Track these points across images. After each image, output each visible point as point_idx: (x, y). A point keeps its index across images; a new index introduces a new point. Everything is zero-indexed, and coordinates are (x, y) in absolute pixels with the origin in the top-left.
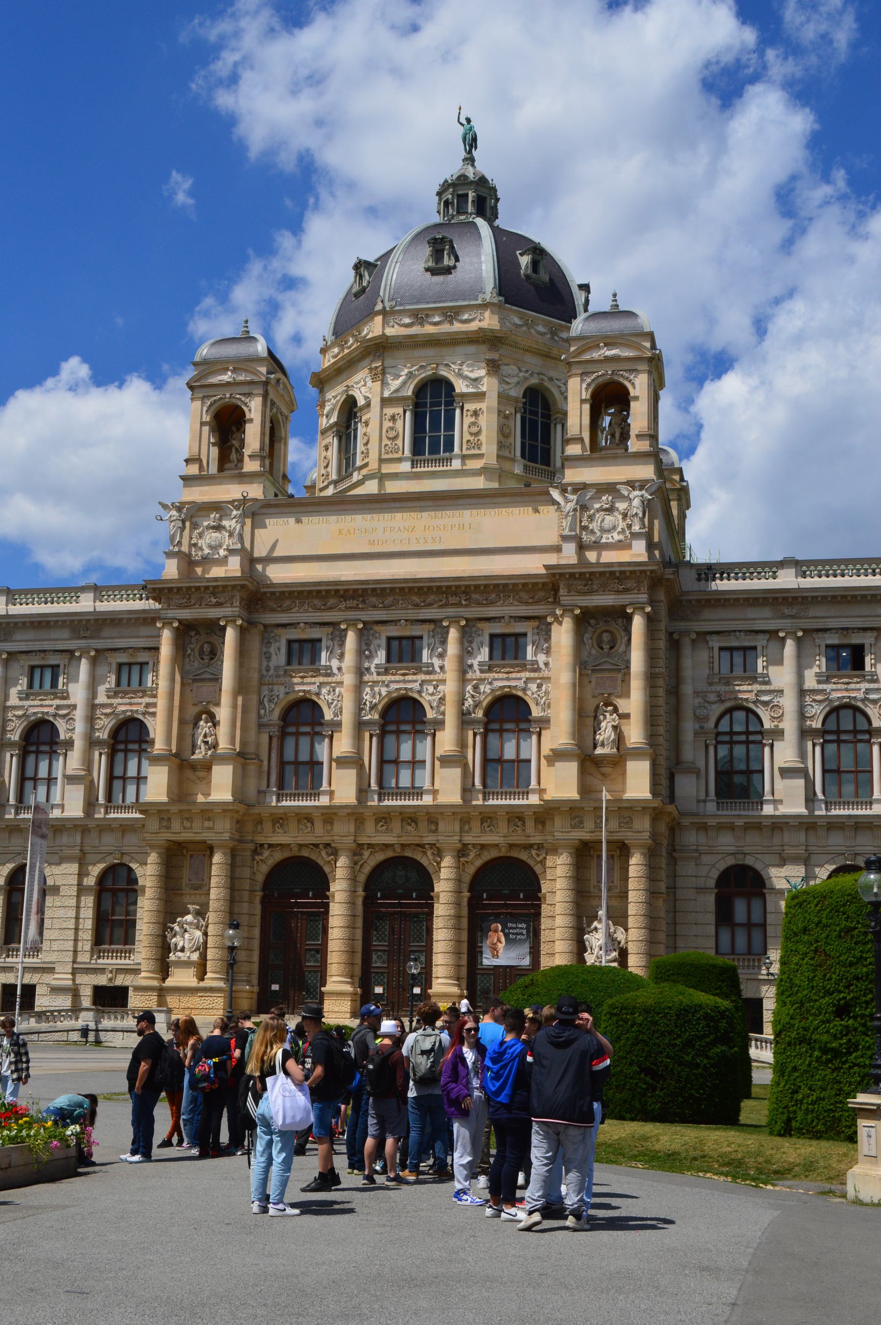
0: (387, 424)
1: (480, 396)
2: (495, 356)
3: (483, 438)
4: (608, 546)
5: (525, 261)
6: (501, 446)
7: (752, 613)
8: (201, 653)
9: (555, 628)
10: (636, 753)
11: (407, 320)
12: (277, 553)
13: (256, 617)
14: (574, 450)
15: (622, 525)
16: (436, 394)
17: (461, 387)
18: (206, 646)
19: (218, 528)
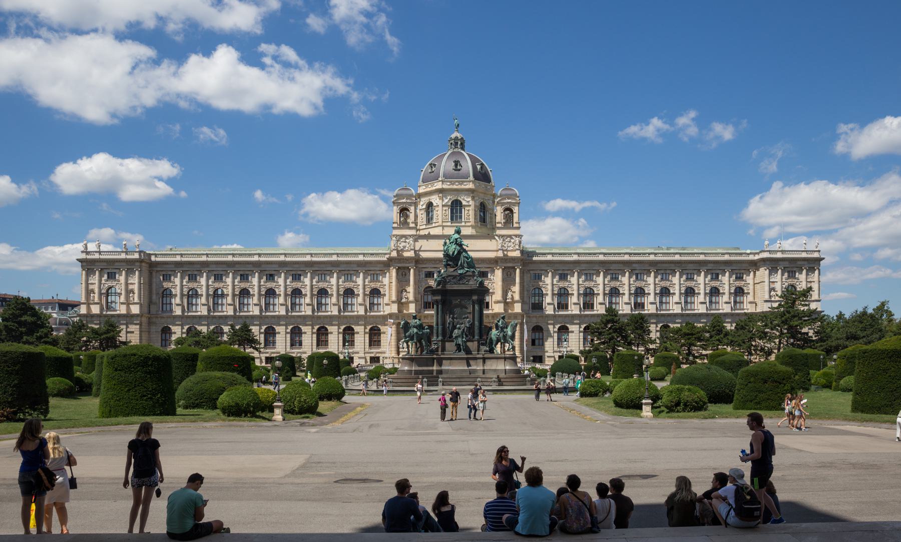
0: (444, 212)
1: (469, 206)
2: (473, 195)
3: (470, 217)
4: (509, 251)
5: (479, 167)
6: (475, 219)
7: (541, 265)
8: (402, 274)
9: (496, 270)
10: (517, 302)
11: (448, 184)
12: (422, 249)
13: (418, 265)
14: (498, 225)
15: (513, 246)
16: (457, 204)
17: (464, 203)
18: (404, 273)
19: (405, 242)
